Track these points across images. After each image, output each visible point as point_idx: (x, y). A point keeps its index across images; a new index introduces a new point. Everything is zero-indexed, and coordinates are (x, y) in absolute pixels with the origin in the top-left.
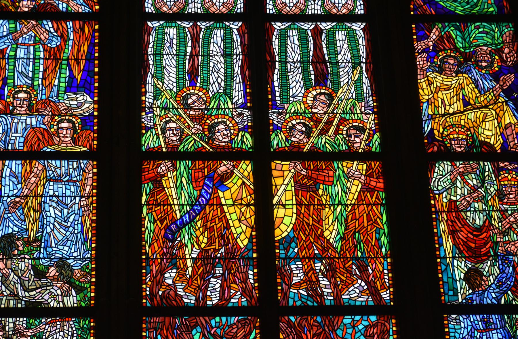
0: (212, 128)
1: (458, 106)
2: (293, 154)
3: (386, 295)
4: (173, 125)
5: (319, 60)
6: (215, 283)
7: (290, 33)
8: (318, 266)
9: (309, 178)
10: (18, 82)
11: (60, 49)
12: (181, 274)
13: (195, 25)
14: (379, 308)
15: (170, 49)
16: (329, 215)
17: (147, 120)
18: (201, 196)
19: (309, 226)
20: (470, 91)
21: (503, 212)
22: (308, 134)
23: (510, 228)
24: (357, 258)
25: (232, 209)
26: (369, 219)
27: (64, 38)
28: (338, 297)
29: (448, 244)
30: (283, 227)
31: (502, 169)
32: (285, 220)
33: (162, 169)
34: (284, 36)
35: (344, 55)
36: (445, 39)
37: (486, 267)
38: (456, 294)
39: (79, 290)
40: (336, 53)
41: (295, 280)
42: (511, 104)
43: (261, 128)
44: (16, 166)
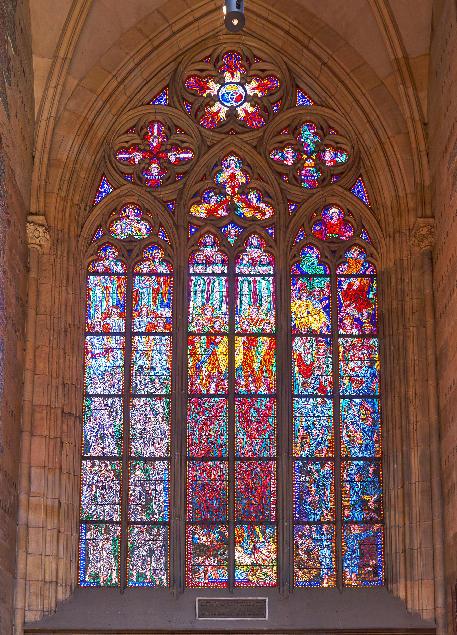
0: (214, 322)
1: (306, 314)
2: (243, 334)
3: (273, 391)
4: (200, 321)
5: (255, 294)
6: (213, 386)
7: (245, 282)
8: (250, 379)
9: (249, 343)
10: (143, 304)
11: (158, 289)
12: (201, 382)
13: (209, 278)
14: (270, 396)
15: (199, 289)
16: (254, 358)
17: (190, 319)
18: (209, 351)
19: (247, 364)
20: (311, 308)
21: (317, 358)
22: (249, 326)
23: (320, 365)
24: (264, 376)
25: (220, 356)
26: (269, 361)
27: (160, 285)
28: (256, 392)
29: (297, 371)
30: (238, 364)
31: (319, 341)
32: (239, 361)
33: (195, 340)
34: (242, 283)
35: (264, 292)
36: (303, 285)
37: (309, 380)
38: (298, 391)
39: (166, 387)
40: (261, 291)
41: (242, 385)
42: (325, 313)
43: (232, 323)
44: (143, 338)
